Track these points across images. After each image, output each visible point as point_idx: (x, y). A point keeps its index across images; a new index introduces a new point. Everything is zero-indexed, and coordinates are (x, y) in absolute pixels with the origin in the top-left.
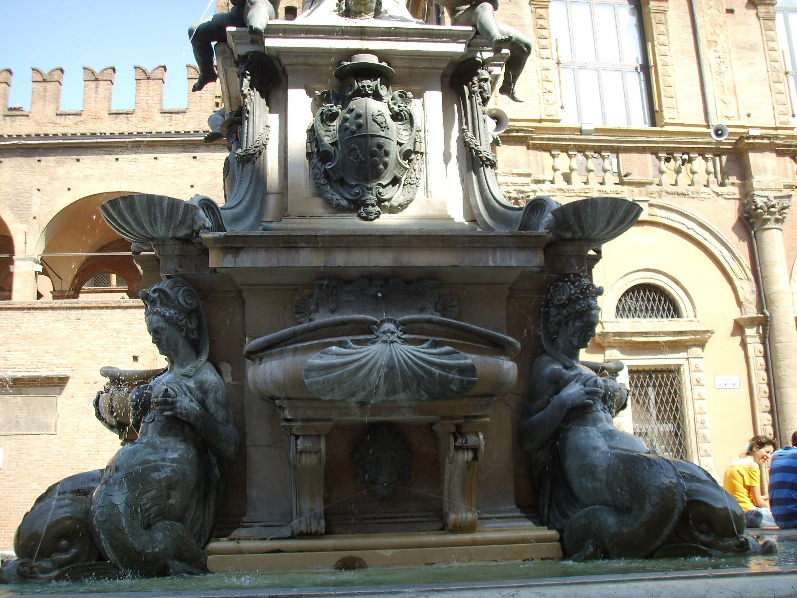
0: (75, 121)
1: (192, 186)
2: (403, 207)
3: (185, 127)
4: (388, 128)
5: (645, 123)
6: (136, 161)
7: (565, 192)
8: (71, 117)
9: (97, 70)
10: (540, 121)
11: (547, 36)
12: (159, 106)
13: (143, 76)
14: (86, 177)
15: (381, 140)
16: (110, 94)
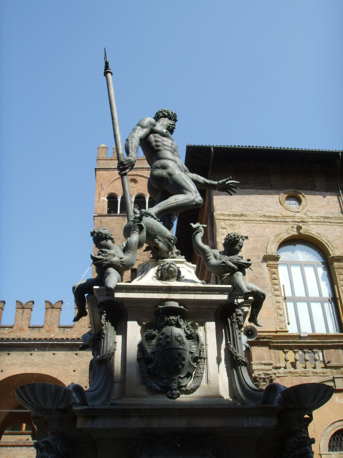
0: (9, 331)
1: (74, 371)
2: (193, 390)
3: (72, 336)
4: (184, 344)
5: (337, 331)
6: (42, 355)
7: (293, 374)
8: (7, 329)
9: (24, 303)
10: (276, 332)
11: (278, 283)
12: (57, 324)
13: (50, 306)
14: (12, 364)
15: (180, 351)
16: (30, 316)
